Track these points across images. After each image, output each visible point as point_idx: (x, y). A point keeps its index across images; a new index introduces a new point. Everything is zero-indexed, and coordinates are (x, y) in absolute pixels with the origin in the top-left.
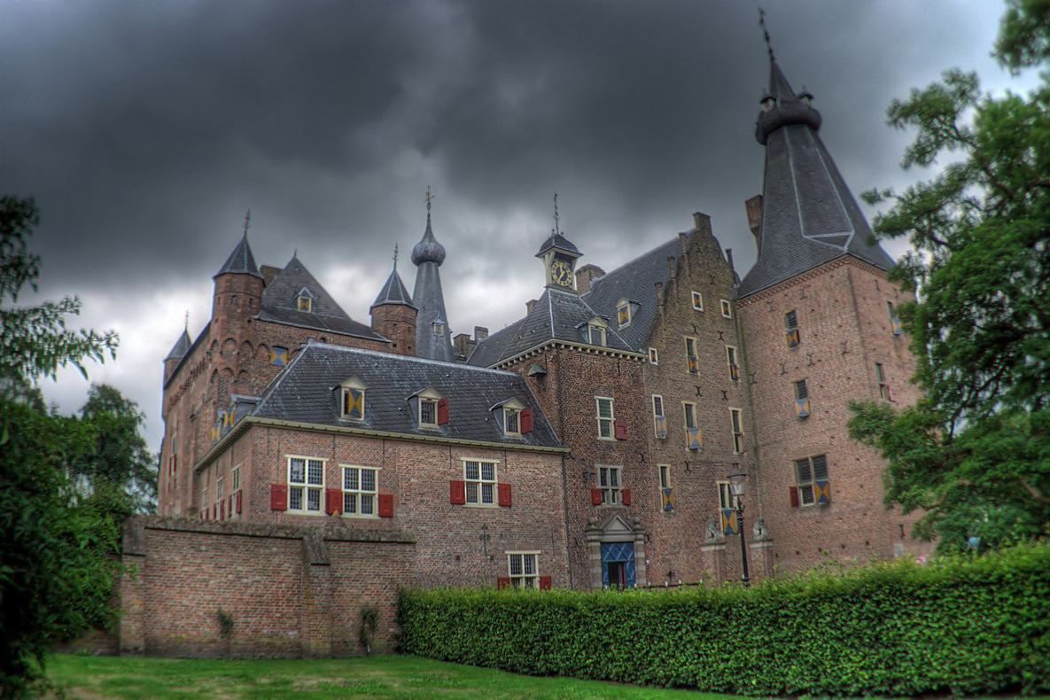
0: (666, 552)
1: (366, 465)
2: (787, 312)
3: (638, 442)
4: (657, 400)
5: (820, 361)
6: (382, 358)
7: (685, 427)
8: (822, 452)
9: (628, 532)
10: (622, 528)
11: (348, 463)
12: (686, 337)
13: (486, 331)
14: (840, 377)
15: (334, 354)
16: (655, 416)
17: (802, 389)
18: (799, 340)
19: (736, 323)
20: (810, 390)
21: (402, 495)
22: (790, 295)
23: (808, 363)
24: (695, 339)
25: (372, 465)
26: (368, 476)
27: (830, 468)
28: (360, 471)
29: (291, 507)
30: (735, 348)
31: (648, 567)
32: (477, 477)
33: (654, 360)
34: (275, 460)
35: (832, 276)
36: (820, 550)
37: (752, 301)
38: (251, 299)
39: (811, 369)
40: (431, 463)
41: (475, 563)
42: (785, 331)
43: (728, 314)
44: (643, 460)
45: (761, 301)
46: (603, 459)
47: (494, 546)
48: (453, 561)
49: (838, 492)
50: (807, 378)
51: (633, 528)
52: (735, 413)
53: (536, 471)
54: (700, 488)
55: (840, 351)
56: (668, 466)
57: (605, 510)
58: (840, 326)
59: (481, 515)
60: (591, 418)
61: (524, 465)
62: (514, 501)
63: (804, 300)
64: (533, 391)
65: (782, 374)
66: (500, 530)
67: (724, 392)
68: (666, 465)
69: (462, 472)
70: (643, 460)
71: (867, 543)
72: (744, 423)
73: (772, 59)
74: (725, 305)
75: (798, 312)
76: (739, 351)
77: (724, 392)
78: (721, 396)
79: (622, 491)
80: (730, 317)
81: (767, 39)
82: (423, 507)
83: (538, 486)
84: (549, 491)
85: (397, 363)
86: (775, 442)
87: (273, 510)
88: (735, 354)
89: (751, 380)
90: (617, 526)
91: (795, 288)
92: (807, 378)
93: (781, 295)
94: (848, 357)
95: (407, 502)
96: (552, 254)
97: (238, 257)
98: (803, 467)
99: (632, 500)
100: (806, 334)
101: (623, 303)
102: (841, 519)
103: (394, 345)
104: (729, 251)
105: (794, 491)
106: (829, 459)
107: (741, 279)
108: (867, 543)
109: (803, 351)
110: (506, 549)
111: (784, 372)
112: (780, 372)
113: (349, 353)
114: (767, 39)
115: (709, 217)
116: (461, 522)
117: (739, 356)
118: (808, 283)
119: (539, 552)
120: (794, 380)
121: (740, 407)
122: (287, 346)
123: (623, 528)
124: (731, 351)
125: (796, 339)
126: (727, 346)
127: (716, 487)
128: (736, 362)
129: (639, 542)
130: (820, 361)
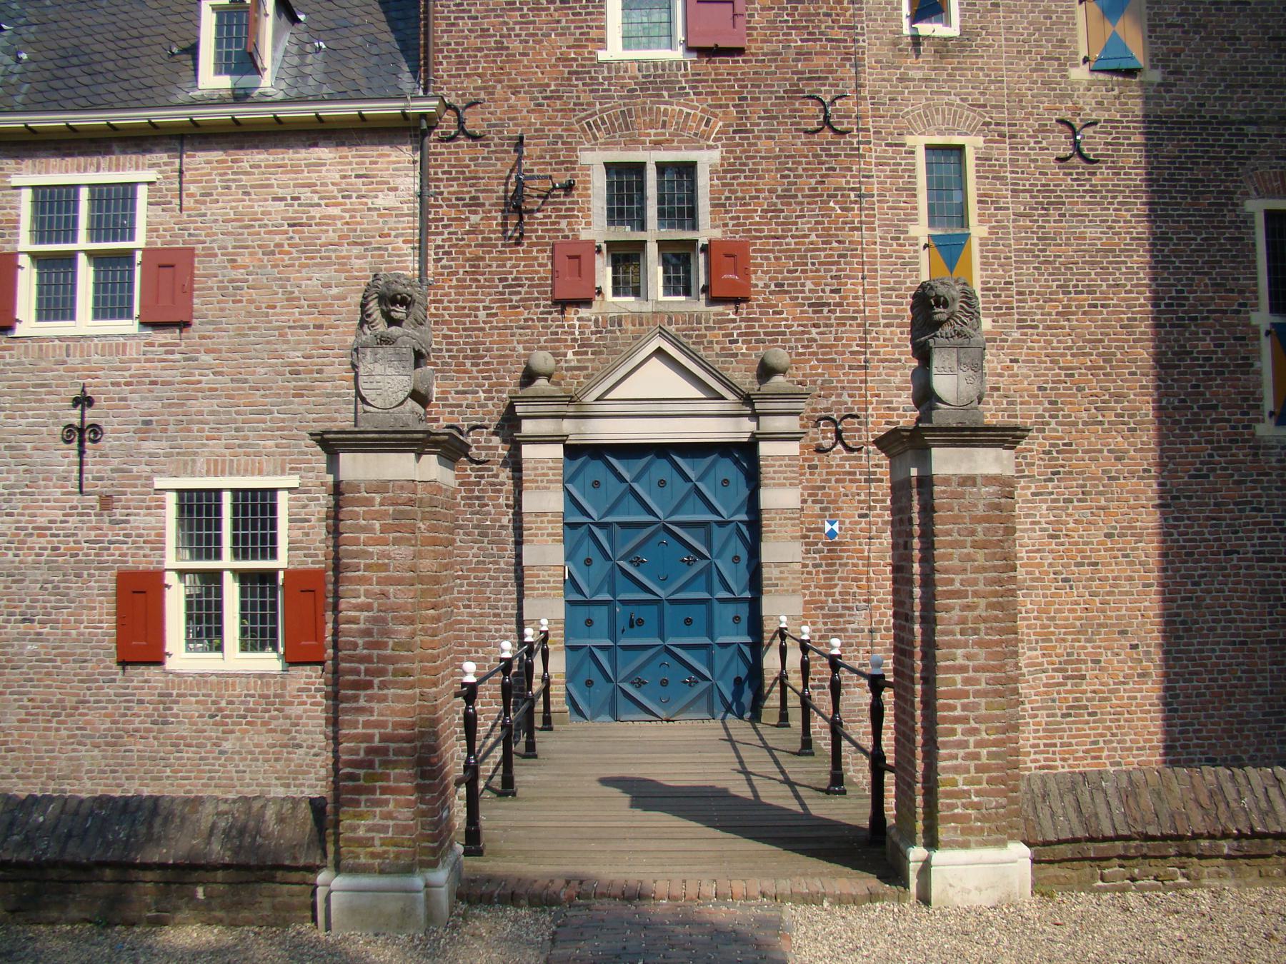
9: (714, 406)
41: (42, 521)
53: (306, 194)
56: (973, 144)
59: (74, 360)
61: (256, 177)
66: (140, 404)
68: (956, 140)
69: (14, 224)
79: (705, 249)
83: (309, 250)
84: (357, 263)
99: (759, 280)
110: (161, 473)
119: (293, 481)
127: (1247, 221)
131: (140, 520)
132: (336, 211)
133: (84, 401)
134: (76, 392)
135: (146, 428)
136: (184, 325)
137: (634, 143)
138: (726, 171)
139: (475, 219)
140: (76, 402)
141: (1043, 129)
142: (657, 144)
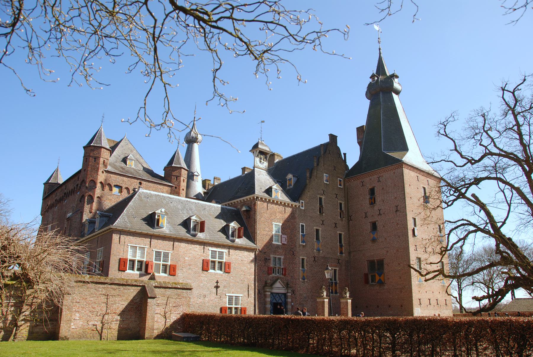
0: (302, 300)
1: (165, 250)
2: (370, 187)
3: (291, 245)
4: (302, 226)
6: (174, 198)
7: (315, 240)
9: (284, 289)
10: (280, 286)
11: (157, 249)
12: (319, 196)
13: (219, 179)
15: (151, 195)
16: (301, 234)
17: (374, 226)
18: (375, 203)
19: (345, 190)
20: (378, 228)
21: (181, 265)
23: (378, 214)
24: (323, 197)
25: (168, 250)
26: (166, 255)
27: (385, 266)
28: (162, 253)
29: (129, 269)
30: (343, 203)
31: (292, 306)
32: (216, 258)
33: (302, 207)
34: (122, 247)
35: (394, 173)
36: (378, 307)
37: (353, 180)
38: (104, 160)
39: (379, 217)
40: (195, 251)
41: (212, 299)
42: (368, 197)
43: (341, 186)
44: (293, 254)
45: (358, 181)
46: (275, 252)
47: (221, 291)
48: (202, 298)
49: (388, 279)
50: (377, 221)
51: (287, 286)
52: (340, 235)
53: (243, 256)
54: (320, 270)
55: (394, 209)
56: (305, 258)
57: (274, 277)
58: (396, 198)
60: (270, 233)
62: (232, 270)
63: (379, 182)
64: (244, 218)
65: (365, 217)
67: (336, 224)
68: (304, 258)
70: (293, 254)
71: (402, 306)
72: (344, 240)
73: (380, 54)
74: (340, 181)
76: (345, 204)
77: (336, 224)
78: (334, 225)
80: (342, 187)
81: (379, 42)
82: (190, 271)
85: (181, 201)
86: (359, 250)
87: (119, 270)
88: (343, 205)
89: (349, 219)
90: (278, 285)
91: (377, 176)
92: (377, 221)
93: (368, 179)
94: (398, 213)
95: (183, 268)
96: (258, 151)
97: (97, 138)
98: (372, 264)
100: (378, 200)
101: (290, 176)
103: (176, 188)
104: (345, 154)
105: (366, 275)
106: (385, 262)
107: (350, 168)
108: (402, 306)
109: (376, 208)
112: (364, 217)
113: (158, 195)
114: (379, 42)
115: (337, 137)
116: (207, 279)
117: (345, 206)
119: (242, 295)
120: (371, 221)
121: (343, 232)
122: (120, 185)
123: (281, 286)
124: (341, 204)
125: (374, 203)
126: (339, 202)
128: (343, 209)
129: (288, 294)
131: (224, 300)
132: (246, 259)
133: (217, 282)
134: (216, 281)
135: (225, 287)
136: (229, 273)
137: (276, 255)
138: (284, 259)
139: (260, 262)
140: (216, 282)
141: (312, 257)
142: (278, 255)
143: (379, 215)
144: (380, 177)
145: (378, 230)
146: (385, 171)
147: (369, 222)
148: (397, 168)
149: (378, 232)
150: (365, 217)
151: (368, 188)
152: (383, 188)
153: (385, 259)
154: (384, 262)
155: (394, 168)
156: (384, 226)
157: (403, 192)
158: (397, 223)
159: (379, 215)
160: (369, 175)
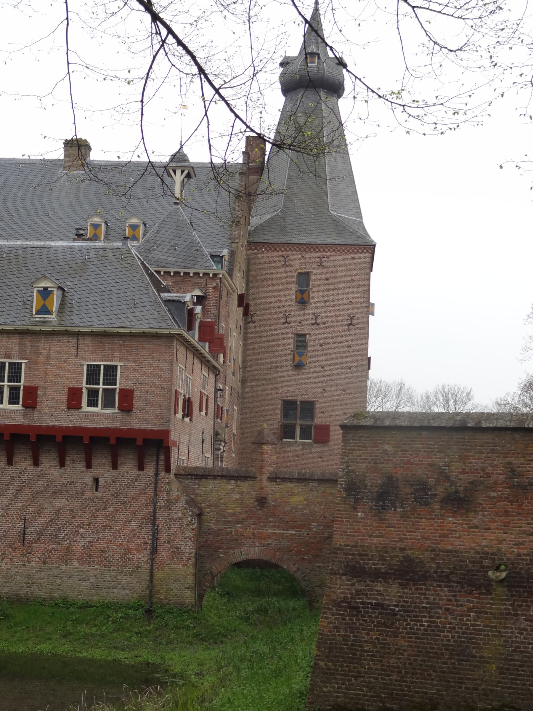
5: (324, 323)
8: (311, 399)
14: (341, 343)
22: (308, 258)
23: (313, 322)
37: (266, 249)
39: (314, 327)
42: (294, 287)
50: (310, 334)
55: (346, 321)
58: (351, 302)
63: (321, 268)
65: (284, 323)
75: (312, 276)
86: (265, 379)
91: (317, 255)
92: (310, 334)
102: (321, 458)
106: (318, 406)
109: (309, 310)
111: (286, 322)
112: (282, 321)
118: (328, 254)
120: (295, 331)
130: (324, 323)
143: (313, 324)
144: (324, 257)
145: (309, 349)
146: (336, 250)
147: (292, 333)
148: (360, 251)
149: (308, 354)
150: (284, 323)
151: (295, 272)
152: (327, 279)
153: (318, 401)
154: (316, 407)
155: (350, 250)
156: (321, 345)
157: (366, 296)
158: (349, 346)
159: (313, 324)
160: (302, 249)
